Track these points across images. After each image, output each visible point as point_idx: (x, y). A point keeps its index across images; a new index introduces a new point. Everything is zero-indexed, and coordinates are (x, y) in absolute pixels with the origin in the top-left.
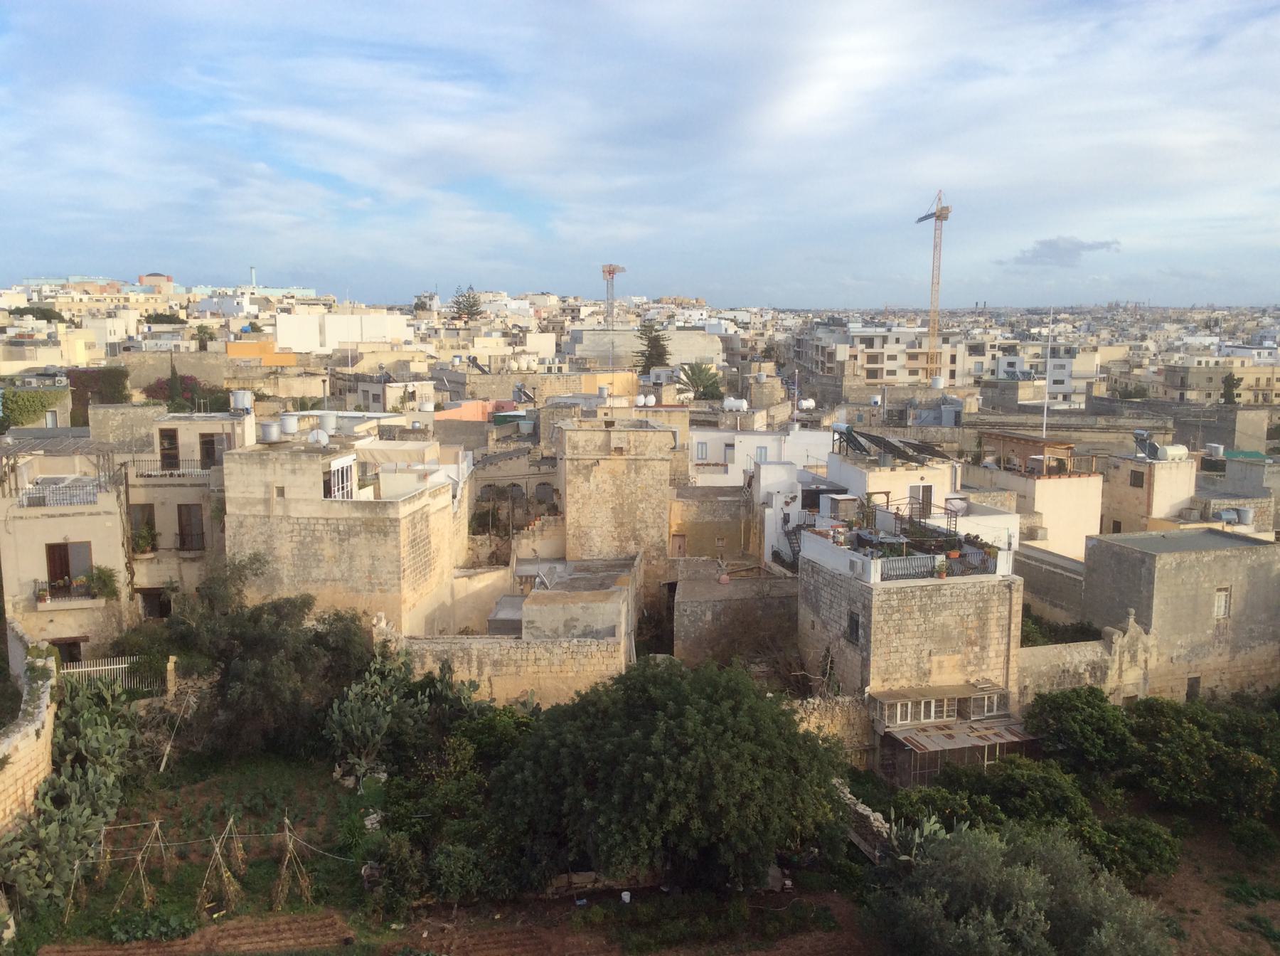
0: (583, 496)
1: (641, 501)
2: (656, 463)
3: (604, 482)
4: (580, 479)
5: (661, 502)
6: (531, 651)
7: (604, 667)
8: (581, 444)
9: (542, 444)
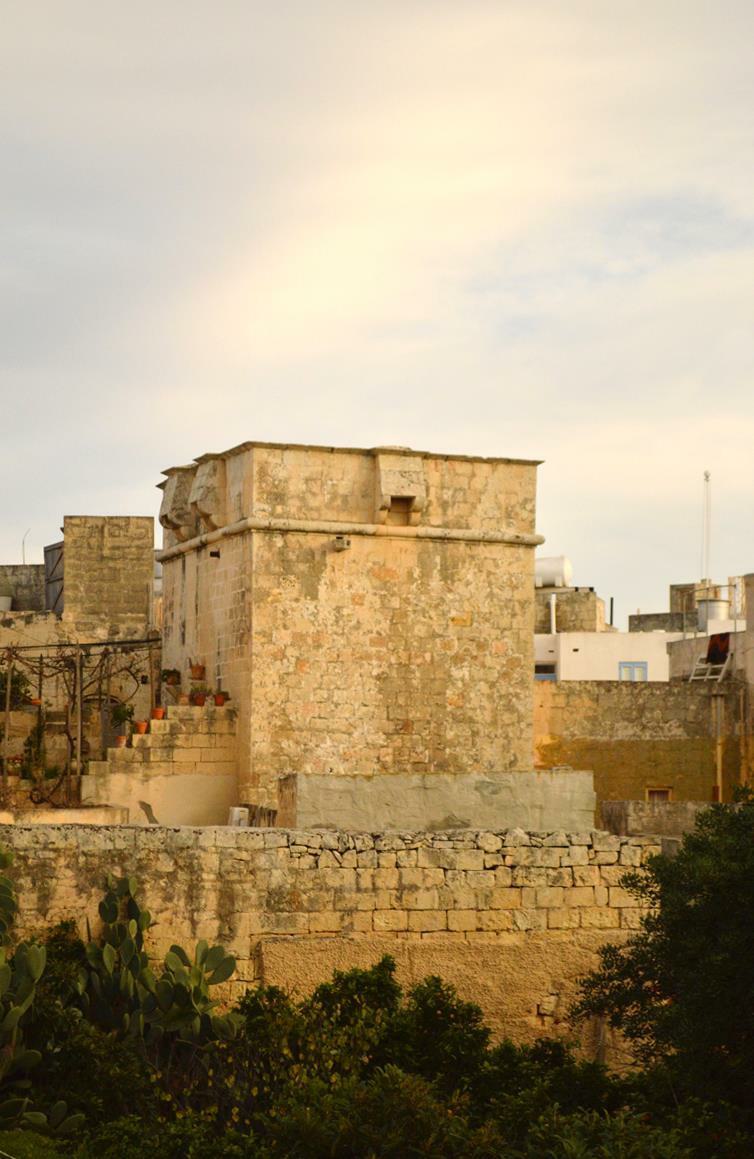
0: (299, 639)
1: (458, 660)
2: (496, 551)
3: (357, 600)
4: (289, 591)
5: (513, 663)
6: (388, 860)
7: (610, 918)
8: (296, 487)
9: (69, 616)
